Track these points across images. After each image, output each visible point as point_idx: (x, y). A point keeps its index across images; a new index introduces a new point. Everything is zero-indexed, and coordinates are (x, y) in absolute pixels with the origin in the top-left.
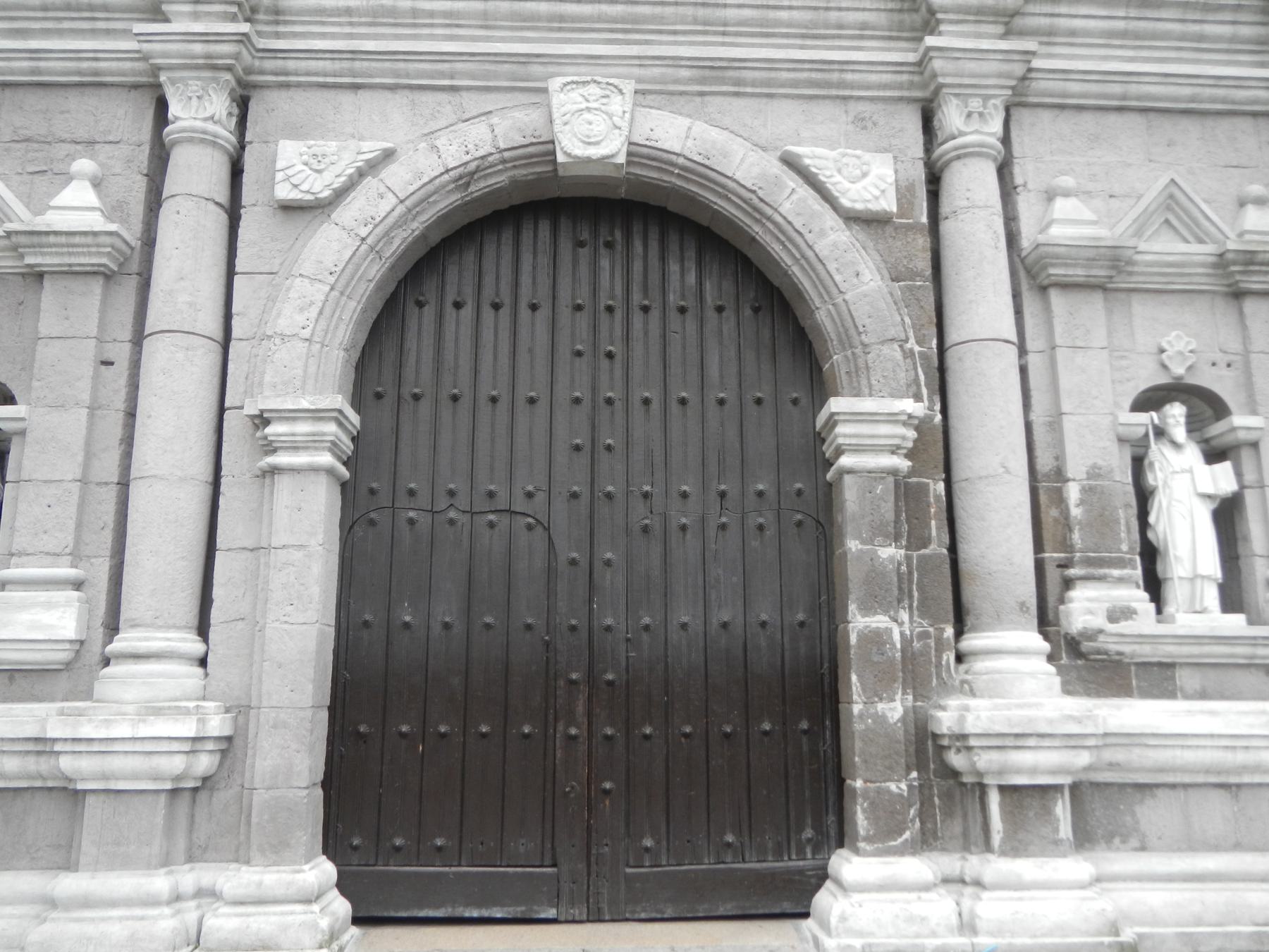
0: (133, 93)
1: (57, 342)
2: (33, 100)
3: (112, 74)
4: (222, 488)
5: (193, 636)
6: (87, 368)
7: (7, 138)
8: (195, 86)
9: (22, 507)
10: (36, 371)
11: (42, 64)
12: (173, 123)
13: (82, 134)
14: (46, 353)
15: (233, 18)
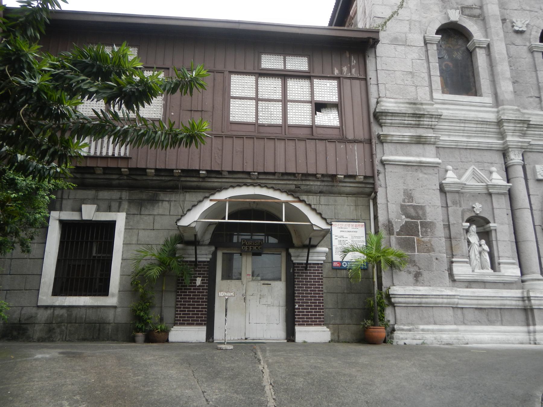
0: (498, 152)
1: (498, 209)
2: (477, 152)
3: (494, 147)
4: (539, 243)
5: (540, 275)
6: (506, 215)
7: (473, 161)
8: (517, 152)
9: (499, 246)
10: (495, 216)
11: (480, 145)
12: (511, 160)
13: (490, 161)
14: (496, 212)
15: (519, 136)
